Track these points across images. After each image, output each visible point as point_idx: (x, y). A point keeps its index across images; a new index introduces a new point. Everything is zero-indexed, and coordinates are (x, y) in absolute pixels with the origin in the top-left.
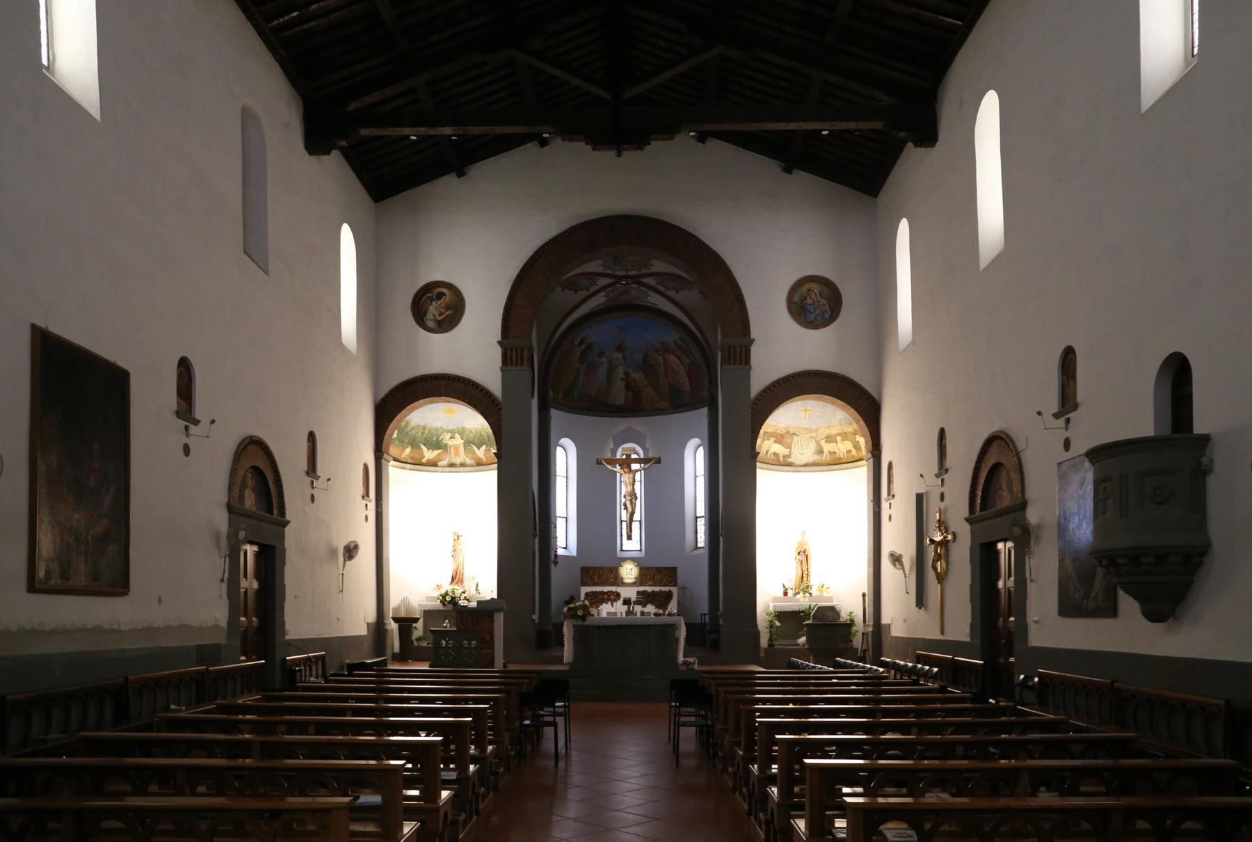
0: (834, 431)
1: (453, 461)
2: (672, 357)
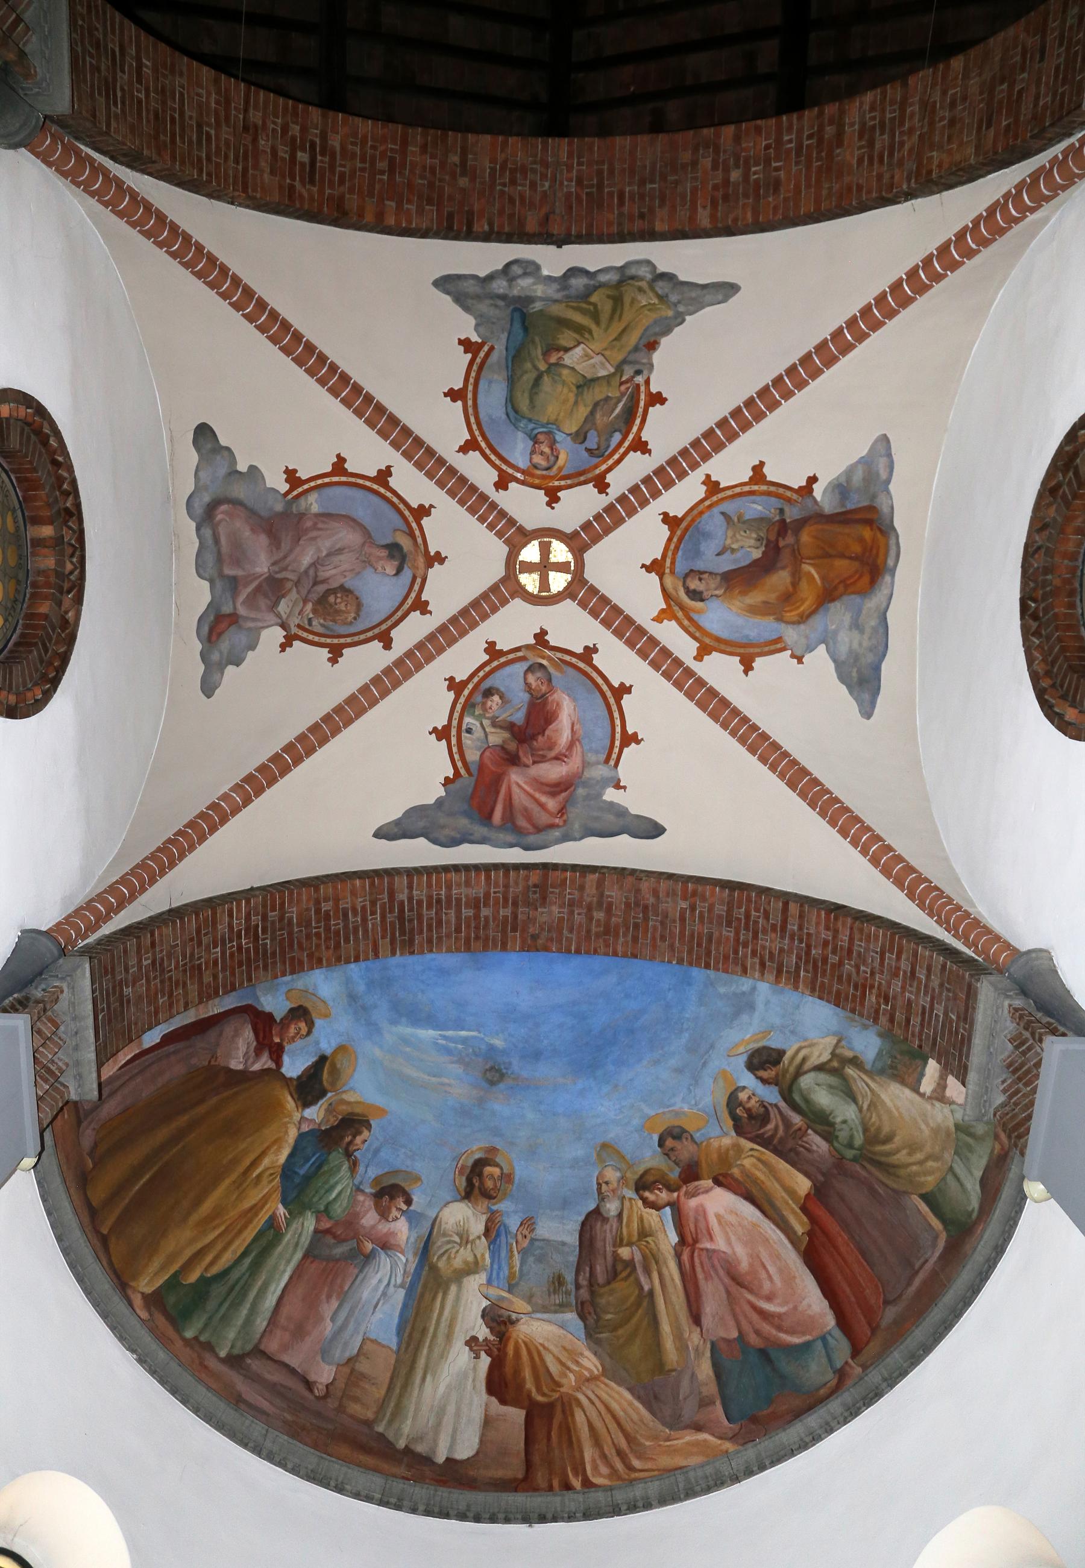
2: (717, 1203)
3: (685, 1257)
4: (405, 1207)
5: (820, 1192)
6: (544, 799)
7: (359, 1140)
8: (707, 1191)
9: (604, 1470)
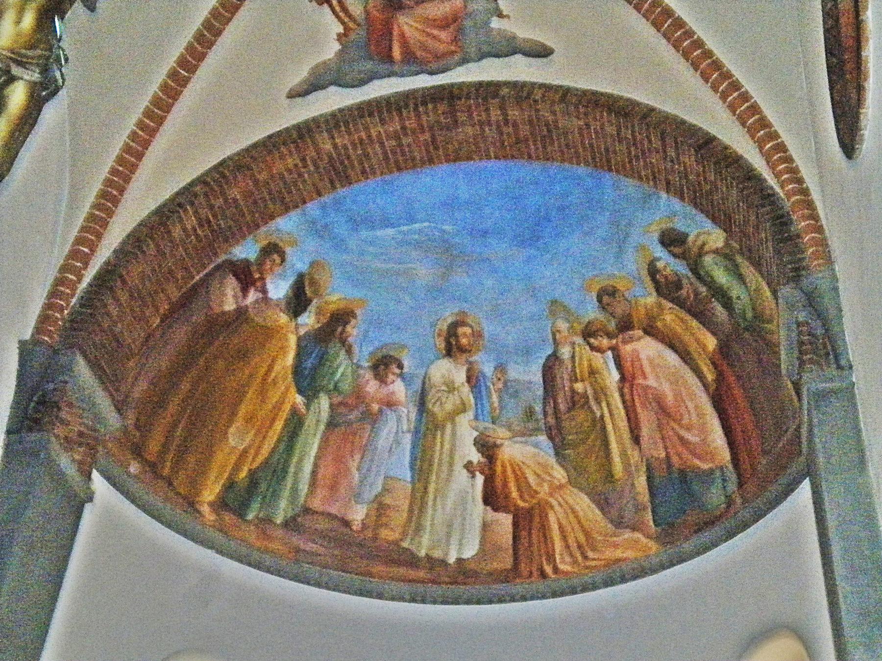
2: (647, 349)
3: (626, 390)
4: (397, 371)
5: (724, 349)
6: (435, 32)
7: (349, 328)
8: (639, 339)
9: (568, 559)
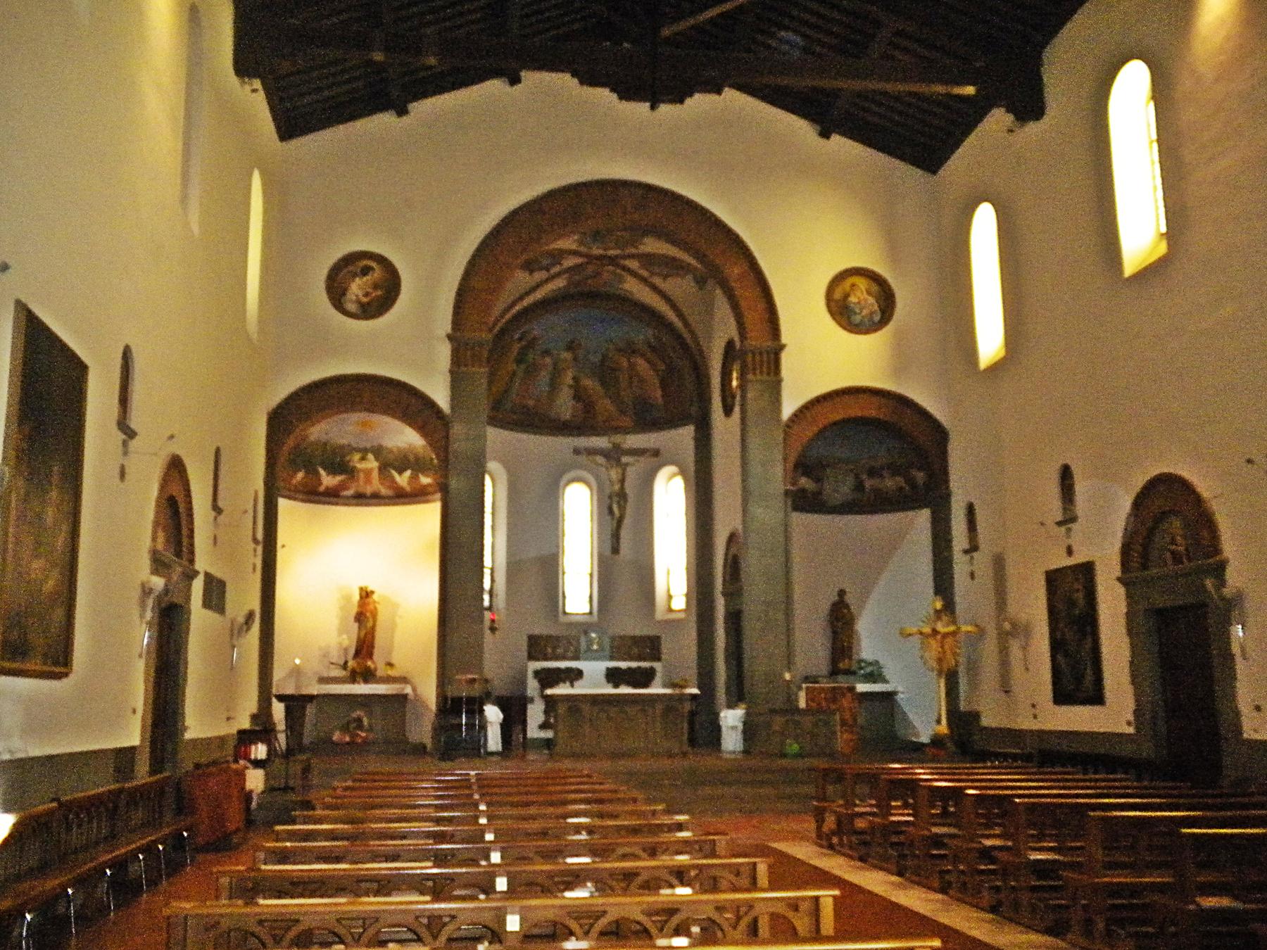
0: (878, 464)
1: (361, 490)
